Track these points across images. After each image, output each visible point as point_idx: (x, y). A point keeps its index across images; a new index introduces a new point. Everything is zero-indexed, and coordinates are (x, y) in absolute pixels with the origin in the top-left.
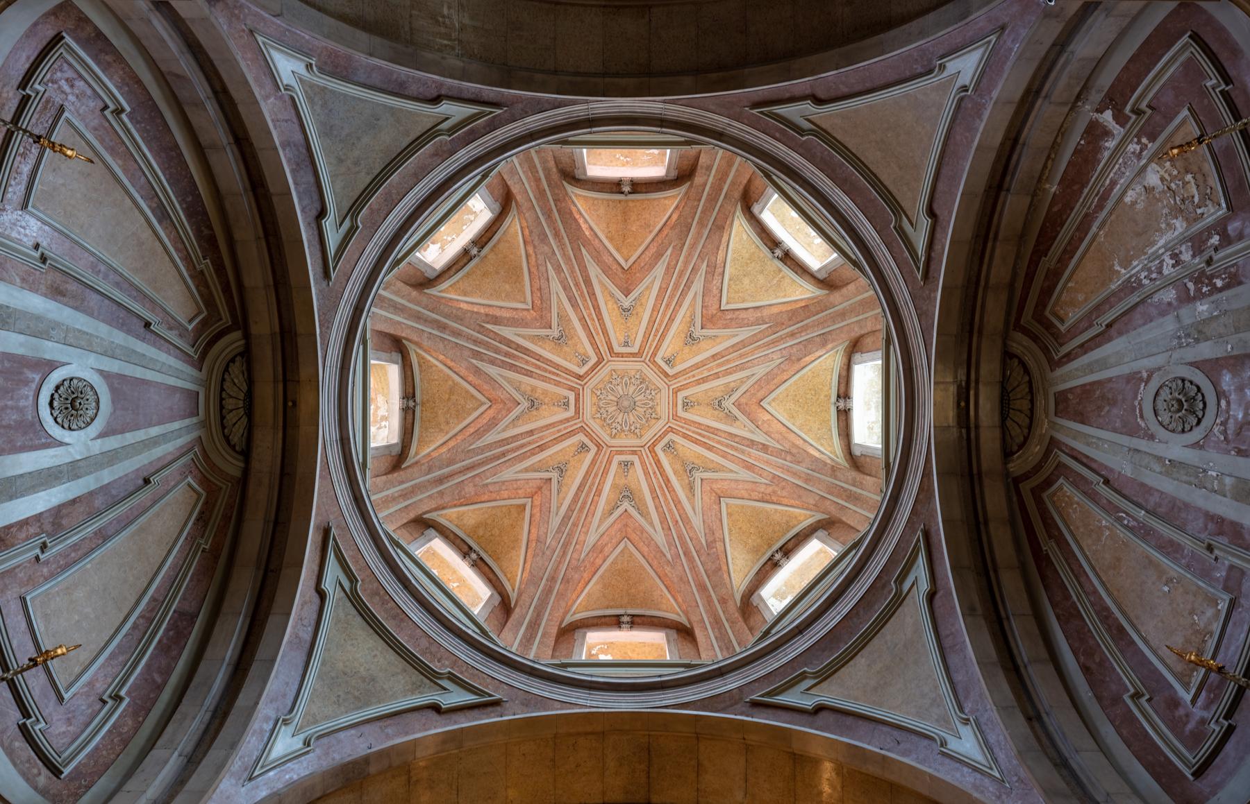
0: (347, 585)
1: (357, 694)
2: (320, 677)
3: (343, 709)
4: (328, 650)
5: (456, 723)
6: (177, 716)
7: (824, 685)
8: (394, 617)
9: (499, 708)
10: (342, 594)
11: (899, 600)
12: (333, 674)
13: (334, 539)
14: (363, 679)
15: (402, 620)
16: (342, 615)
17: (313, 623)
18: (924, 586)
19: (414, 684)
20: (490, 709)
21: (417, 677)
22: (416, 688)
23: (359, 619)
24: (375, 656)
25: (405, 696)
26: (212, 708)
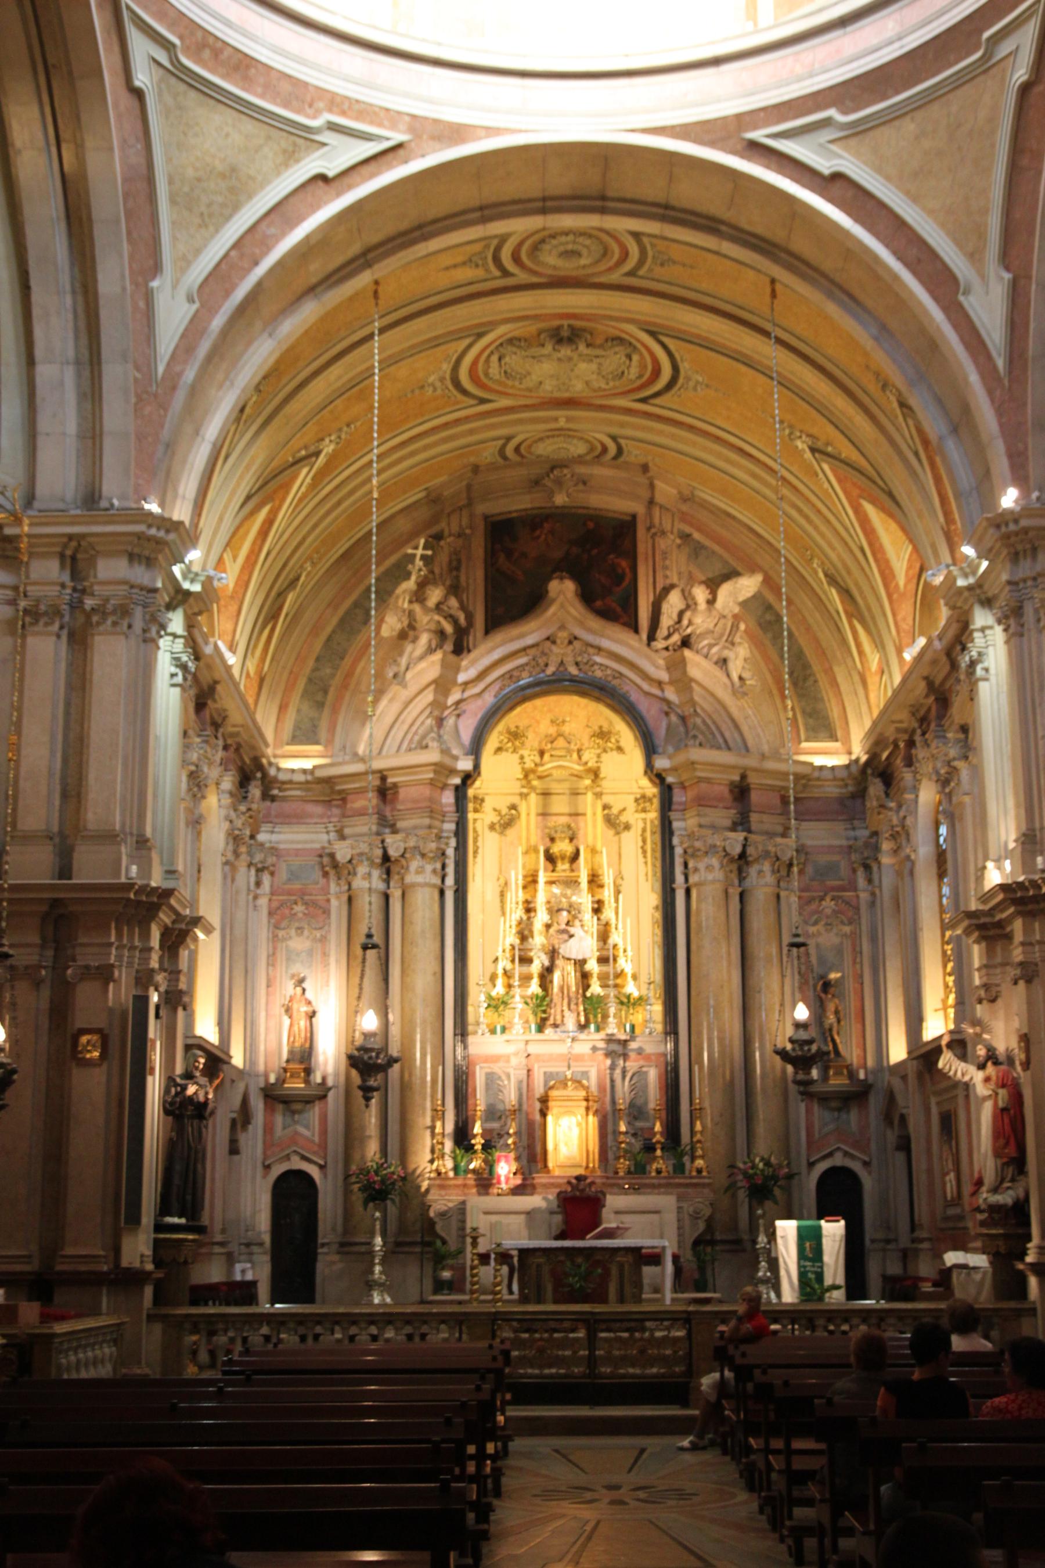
0: (163, 58)
1: (220, 199)
2: (173, 201)
3: (211, 229)
4: (169, 160)
5: (350, 187)
6: (36, 312)
7: (853, 142)
8: (236, 68)
9: (401, 152)
10: (161, 71)
11: (985, 67)
12: (186, 189)
13: (128, 7)
14: (223, 176)
15: (248, 67)
16: (169, 100)
17: (141, 134)
18: (1021, 74)
19: (285, 151)
20: (390, 156)
21: (285, 142)
22: (290, 157)
23: (193, 94)
24: (227, 135)
25: (279, 174)
26: (68, 288)
